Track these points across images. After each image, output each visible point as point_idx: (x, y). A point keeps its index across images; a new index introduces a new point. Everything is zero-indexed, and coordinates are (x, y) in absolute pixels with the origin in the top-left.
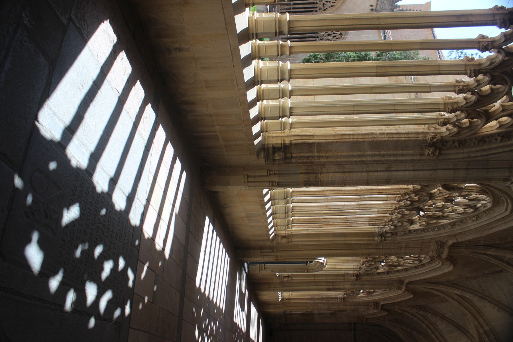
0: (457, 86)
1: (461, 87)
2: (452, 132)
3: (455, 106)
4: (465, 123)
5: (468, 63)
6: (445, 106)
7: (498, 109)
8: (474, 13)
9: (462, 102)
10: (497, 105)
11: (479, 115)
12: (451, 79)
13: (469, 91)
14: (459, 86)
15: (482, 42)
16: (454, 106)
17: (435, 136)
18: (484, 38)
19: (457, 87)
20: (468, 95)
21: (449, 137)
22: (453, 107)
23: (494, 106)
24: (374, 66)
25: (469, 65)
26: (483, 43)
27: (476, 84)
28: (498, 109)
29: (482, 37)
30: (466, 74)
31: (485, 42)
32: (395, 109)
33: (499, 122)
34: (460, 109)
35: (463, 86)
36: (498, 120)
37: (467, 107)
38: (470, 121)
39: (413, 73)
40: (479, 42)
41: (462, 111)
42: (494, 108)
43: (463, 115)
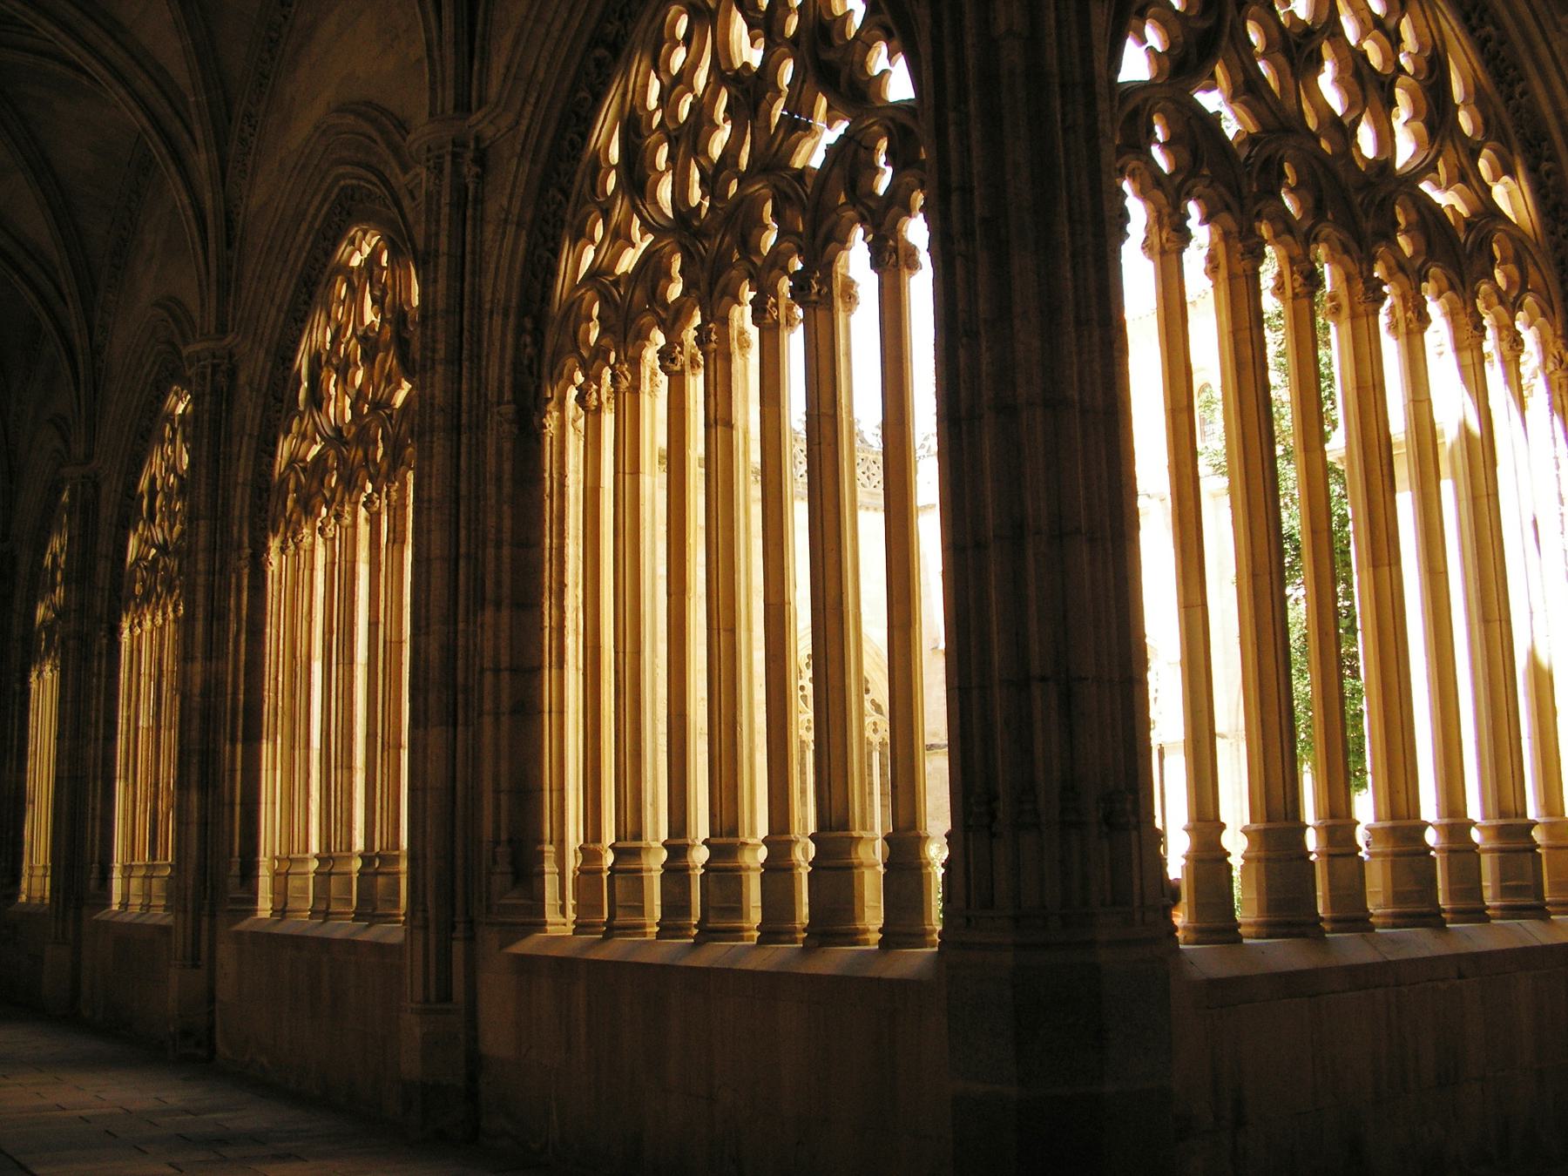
0: (1407, 326)
1: (1409, 314)
2: (1537, 309)
3: (1463, 319)
4: (1508, 277)
5: (1346, 311)
6: (1466, 348)
7: (1457, 193)
8: (1227, 328)
9: (1449, 301)
10: (1447, 199)
11: (1483, 245)
12: (1391, 350)
13: (1419, 291)
14: (1408, 322)
15: (1293, 289)
16: (1464, 322)
17: (1555, 357)
18: (1283, 283)
19: (1411, 326)
20: (1428, 289)
21: (1554, 314)
22: (1467, 324)
23: (1452, 207)
24: (1371, 572)
25: (1352, 308)
26: (1296, 285)
27: (1400, 276)
28: (1458, 192)
29: (1279, 289)
30: (1376, 313)
31: (1293, 281)
32: (1488, 495)
33: (1496, 179)
34: (1469, 303)
35: (1406, 309)
36: (1490, 184)
37: (1463, 283)
38: (1499, 265)
39: (1384, 462)
40: (1295, 296)
41: (1475, 295)
42: (1457, 208)
43: (1484, 287)
